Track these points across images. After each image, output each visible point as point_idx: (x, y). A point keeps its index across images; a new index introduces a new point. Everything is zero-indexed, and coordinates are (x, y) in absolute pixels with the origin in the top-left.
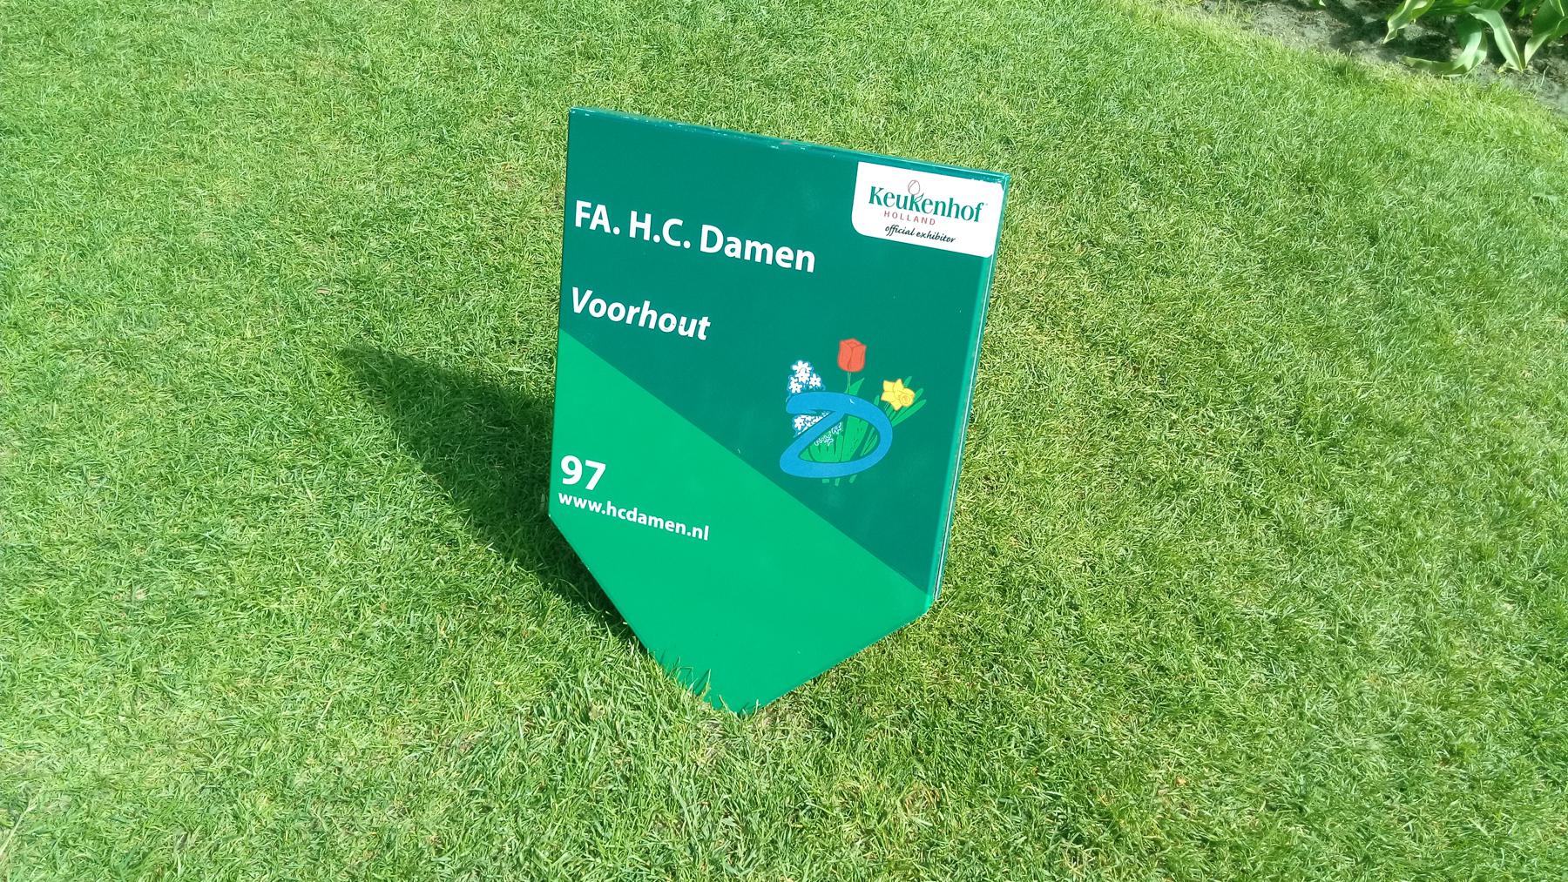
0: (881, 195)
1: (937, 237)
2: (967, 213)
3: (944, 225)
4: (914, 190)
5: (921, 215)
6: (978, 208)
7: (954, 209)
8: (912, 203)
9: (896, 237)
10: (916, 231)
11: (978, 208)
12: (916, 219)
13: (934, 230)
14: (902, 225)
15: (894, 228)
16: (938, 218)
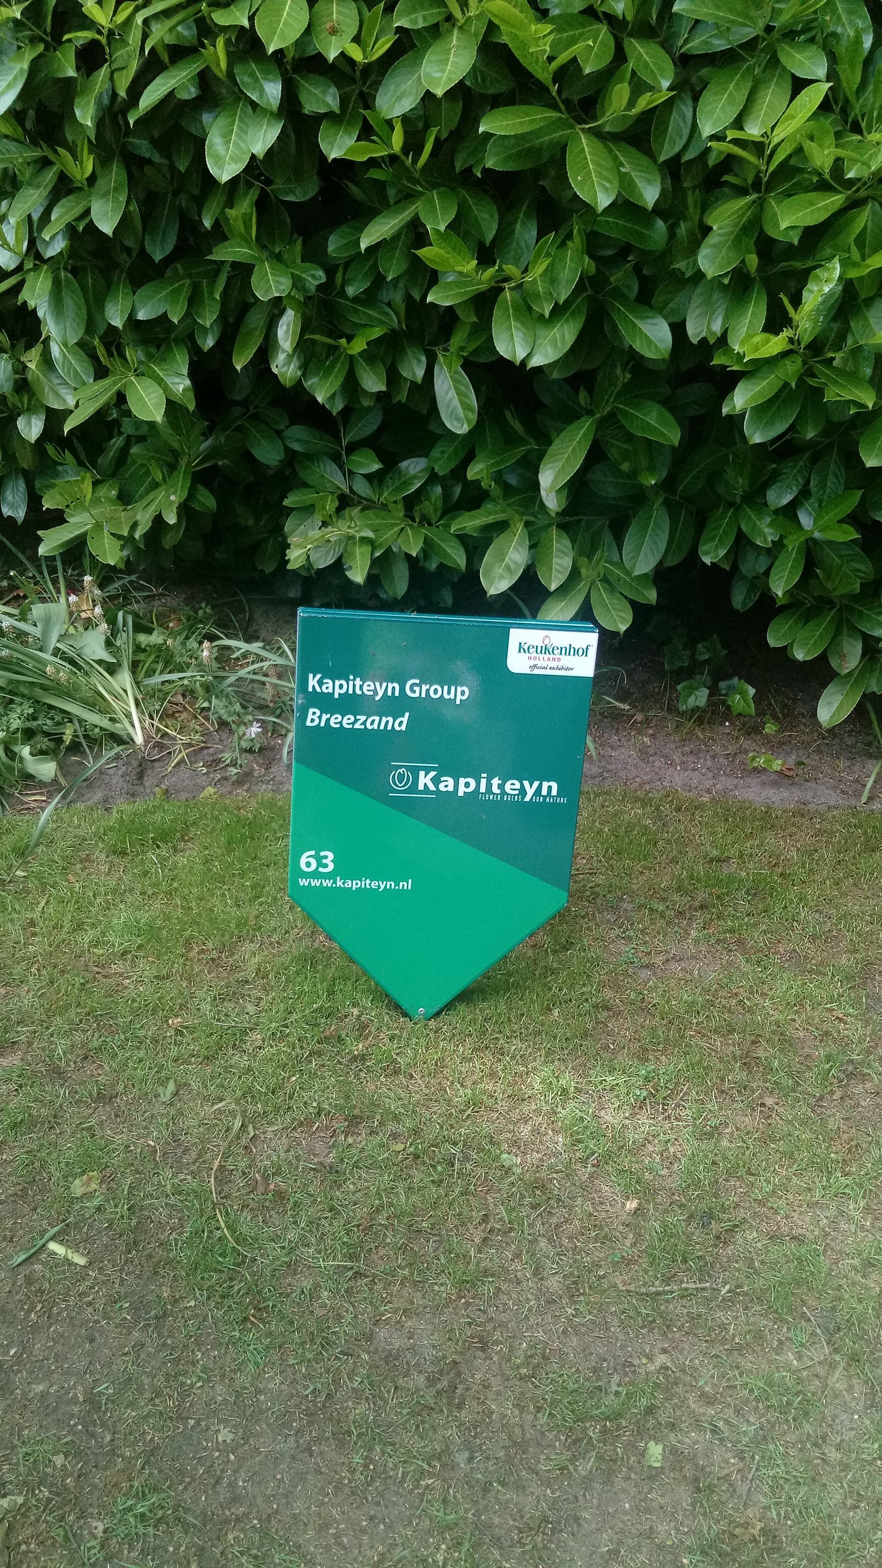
0: (526, 647)
3: (567, 661)
4: (547, 642)
5: (552, 656)
8: (546, 650)
9: (536, 672)
10: (548, 666)
13: (560, 664)
14: (540, 664)
15: (535, 666)
16: (563, 657)
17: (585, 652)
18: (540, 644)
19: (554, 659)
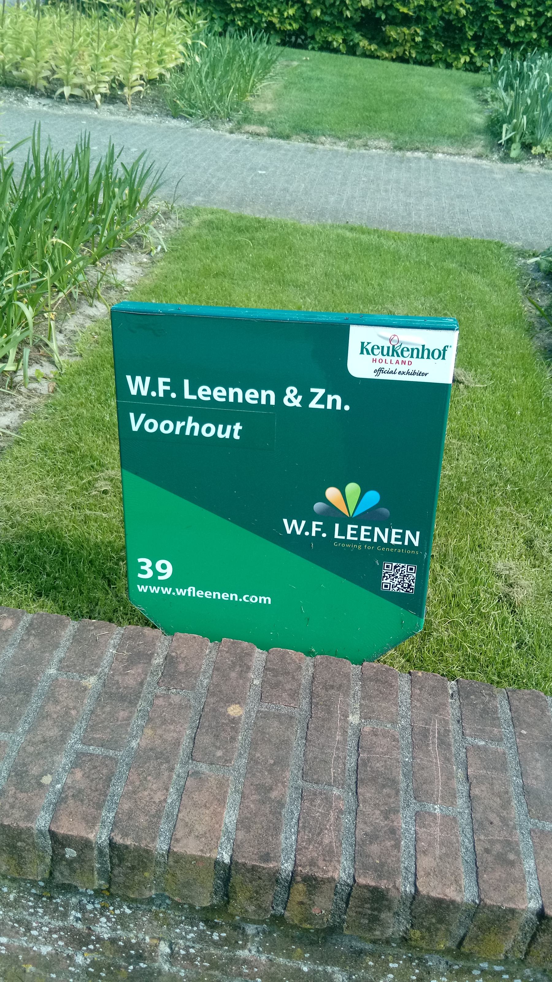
0: (369, 347)
1: (414, 373)
2: (436, 354)
3: (418, 365)
5: (401, 359)
6: (445, 350)
7: (426, 352)
9: (383, 377)
10: (397, 371)
11: (445, 350)
12: (397, 362)
13: (411, 368)
14: (387, 367)
15: (381, 370)
17: (442, 354)
18: (386, 344)
19: (404, 362)
